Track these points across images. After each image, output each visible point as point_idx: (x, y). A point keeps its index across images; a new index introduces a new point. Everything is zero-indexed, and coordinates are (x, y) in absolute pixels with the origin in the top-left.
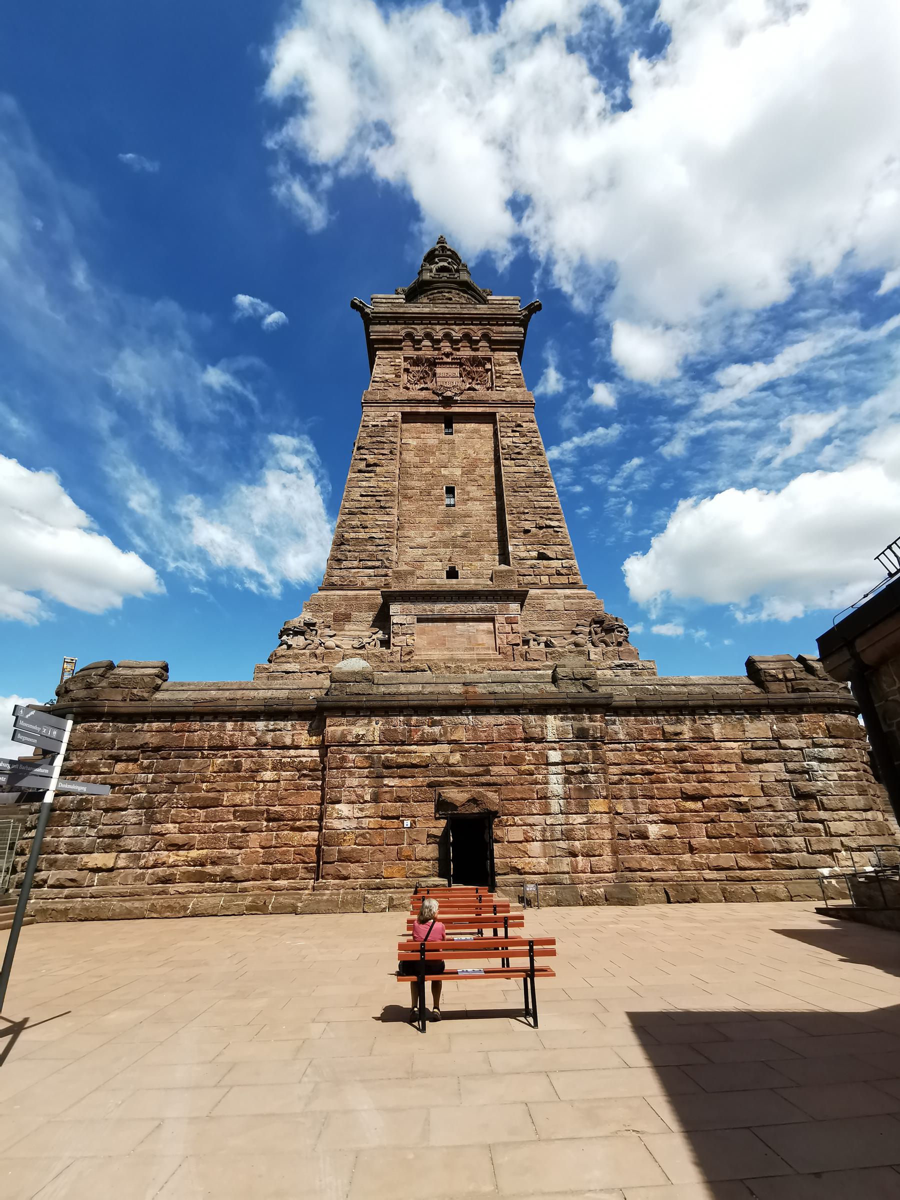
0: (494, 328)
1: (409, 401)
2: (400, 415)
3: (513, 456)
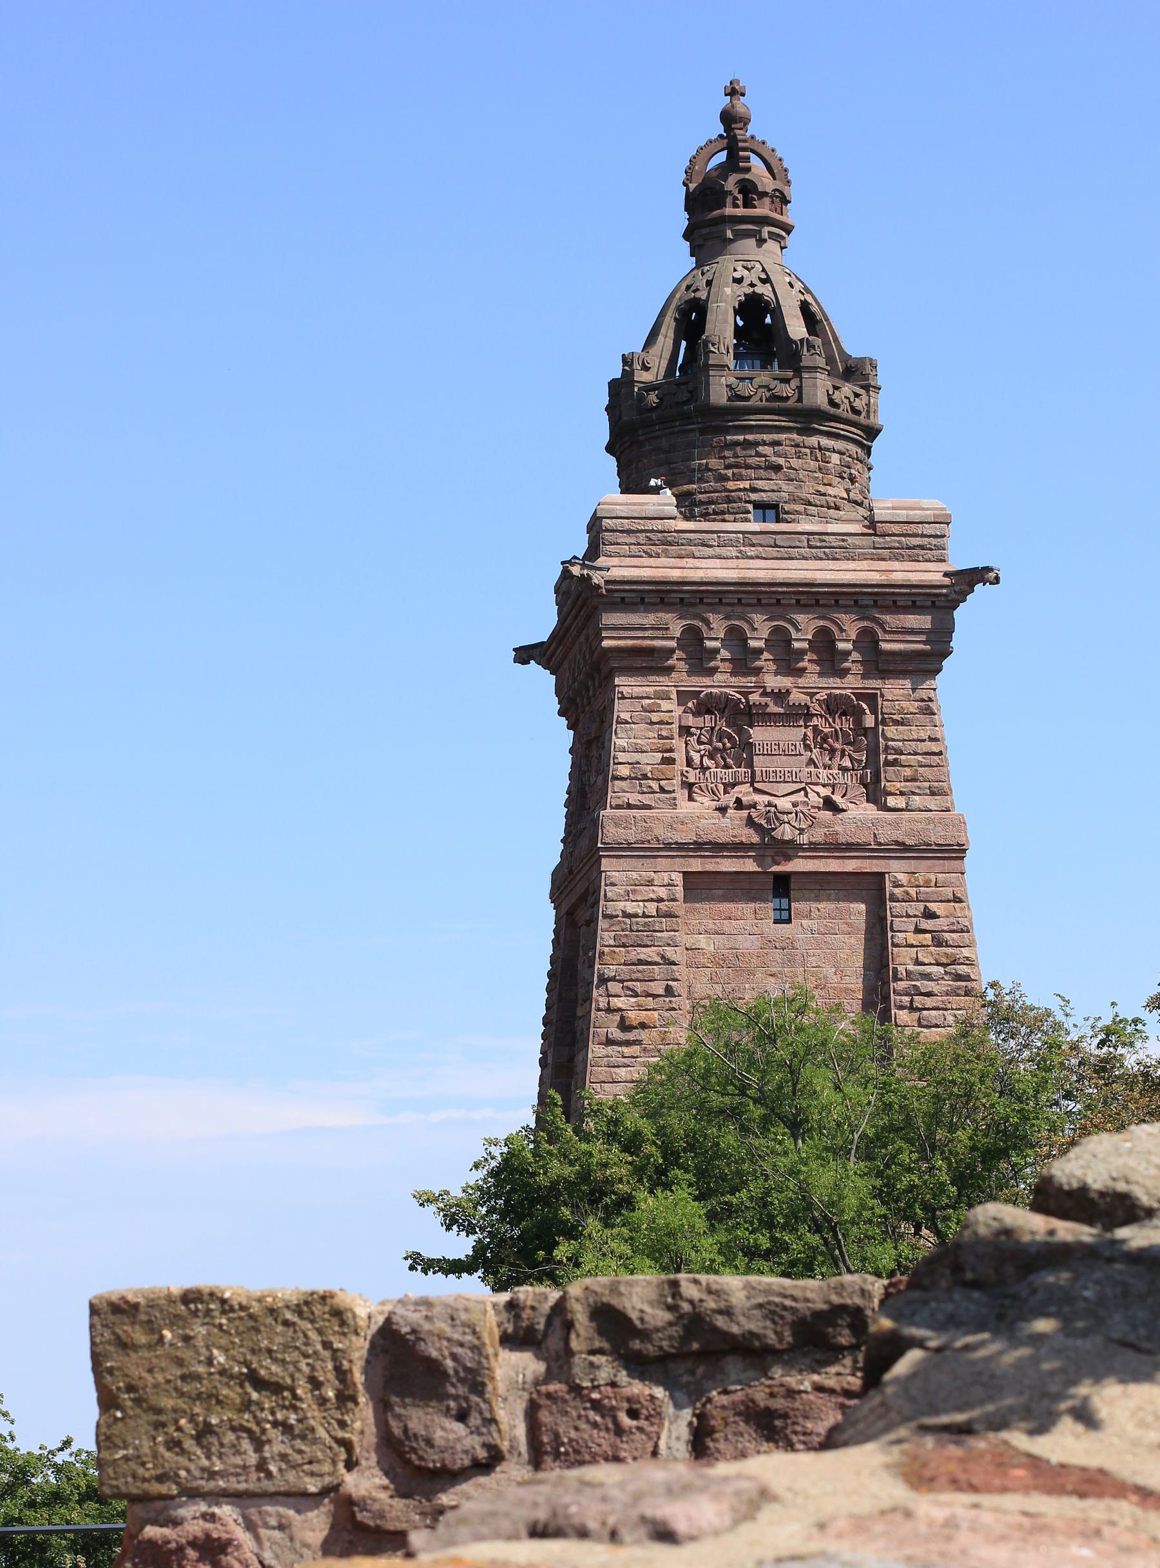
0: (888, 618)
1: (699, 847)
2: (678, 878)
3: (919, 1001)
